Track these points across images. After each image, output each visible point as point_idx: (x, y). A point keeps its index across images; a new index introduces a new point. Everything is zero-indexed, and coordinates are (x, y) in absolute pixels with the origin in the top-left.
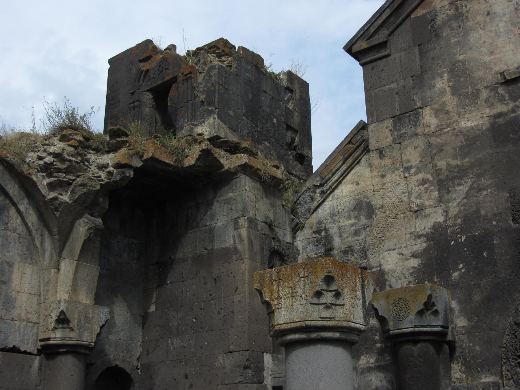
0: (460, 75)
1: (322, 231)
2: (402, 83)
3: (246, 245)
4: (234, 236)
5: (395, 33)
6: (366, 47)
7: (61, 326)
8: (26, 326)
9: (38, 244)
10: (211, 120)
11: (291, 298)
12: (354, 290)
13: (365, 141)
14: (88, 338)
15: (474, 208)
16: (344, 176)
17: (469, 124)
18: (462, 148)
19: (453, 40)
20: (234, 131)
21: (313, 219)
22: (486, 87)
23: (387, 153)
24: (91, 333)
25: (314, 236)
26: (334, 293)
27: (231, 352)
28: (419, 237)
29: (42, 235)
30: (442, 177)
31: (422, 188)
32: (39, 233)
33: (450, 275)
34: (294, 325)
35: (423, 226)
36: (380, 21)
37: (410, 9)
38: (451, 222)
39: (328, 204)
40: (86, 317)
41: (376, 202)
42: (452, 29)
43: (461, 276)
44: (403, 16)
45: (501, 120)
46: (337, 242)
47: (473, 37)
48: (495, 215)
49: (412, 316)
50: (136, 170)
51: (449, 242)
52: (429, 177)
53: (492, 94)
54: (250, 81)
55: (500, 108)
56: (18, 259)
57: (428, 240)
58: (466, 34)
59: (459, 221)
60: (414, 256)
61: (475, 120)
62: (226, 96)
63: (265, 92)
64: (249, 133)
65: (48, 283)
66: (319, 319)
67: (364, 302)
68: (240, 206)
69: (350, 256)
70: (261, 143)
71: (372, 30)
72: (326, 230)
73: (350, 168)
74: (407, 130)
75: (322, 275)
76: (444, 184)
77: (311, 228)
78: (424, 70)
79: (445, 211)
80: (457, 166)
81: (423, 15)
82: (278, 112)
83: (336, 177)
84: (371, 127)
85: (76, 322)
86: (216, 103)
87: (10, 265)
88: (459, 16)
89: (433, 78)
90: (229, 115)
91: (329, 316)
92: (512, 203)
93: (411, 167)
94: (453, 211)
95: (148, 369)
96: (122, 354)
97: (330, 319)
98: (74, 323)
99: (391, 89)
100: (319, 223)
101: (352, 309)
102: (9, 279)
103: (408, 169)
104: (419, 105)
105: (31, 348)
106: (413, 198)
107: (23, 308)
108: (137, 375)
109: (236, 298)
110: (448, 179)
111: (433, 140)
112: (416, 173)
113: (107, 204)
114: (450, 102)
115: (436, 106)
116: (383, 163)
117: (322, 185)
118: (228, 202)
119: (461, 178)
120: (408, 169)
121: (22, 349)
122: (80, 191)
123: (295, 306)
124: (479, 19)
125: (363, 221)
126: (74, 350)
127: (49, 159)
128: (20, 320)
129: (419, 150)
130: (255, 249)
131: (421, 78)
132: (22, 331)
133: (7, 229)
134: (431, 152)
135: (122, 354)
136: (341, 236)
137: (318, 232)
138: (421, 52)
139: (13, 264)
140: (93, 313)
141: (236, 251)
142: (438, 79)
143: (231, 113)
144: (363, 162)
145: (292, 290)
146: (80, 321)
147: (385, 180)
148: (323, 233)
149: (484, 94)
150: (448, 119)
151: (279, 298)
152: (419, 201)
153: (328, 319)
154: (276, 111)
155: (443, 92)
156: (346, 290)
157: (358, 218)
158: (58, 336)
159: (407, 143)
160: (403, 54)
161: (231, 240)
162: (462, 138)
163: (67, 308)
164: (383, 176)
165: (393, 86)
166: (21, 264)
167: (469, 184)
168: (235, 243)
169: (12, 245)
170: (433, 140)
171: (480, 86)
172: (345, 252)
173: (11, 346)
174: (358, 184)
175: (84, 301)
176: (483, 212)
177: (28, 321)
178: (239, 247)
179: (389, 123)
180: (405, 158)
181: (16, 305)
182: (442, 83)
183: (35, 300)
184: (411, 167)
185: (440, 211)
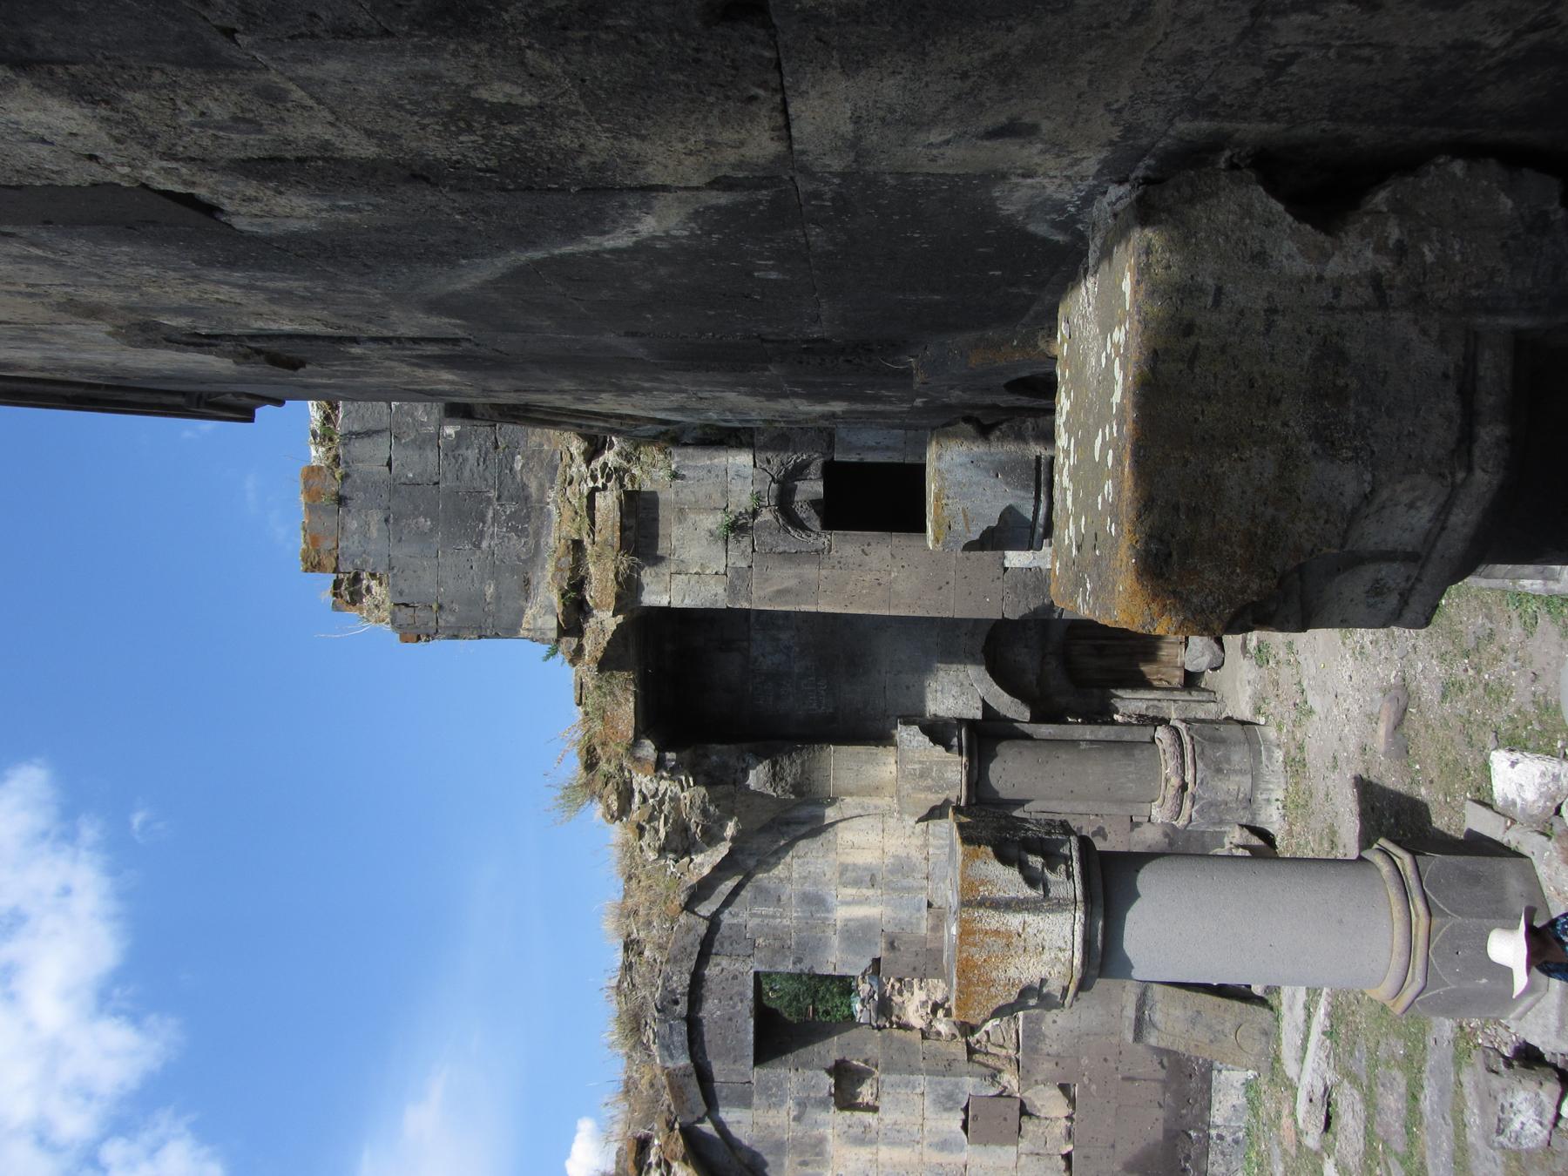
8: (934, 836)
12: (1008, 939)
20: (527, 582)
24: (947, 764)
29: (788, 823)
32: (784, 829)
40: (921, 776)
50: (661, 749)
54: (387, 520)
56: (832, 855)
62: (456, 607)
63: (389, 465)
64: (514, 529)
70: (524, 487)
87: (844, 869)
101: (1046, 957)
102: (866, 869)
107: (906, 842)
113: (719, 747)
128: (926, 845)
130: (792, 583)
133: (789, 879)
140: (912, 762)
143: (490, 590)
146: (929, 789)
154: (422, 424)
156: (1012, 972)
163: (913, 815)
175: (893, 768)
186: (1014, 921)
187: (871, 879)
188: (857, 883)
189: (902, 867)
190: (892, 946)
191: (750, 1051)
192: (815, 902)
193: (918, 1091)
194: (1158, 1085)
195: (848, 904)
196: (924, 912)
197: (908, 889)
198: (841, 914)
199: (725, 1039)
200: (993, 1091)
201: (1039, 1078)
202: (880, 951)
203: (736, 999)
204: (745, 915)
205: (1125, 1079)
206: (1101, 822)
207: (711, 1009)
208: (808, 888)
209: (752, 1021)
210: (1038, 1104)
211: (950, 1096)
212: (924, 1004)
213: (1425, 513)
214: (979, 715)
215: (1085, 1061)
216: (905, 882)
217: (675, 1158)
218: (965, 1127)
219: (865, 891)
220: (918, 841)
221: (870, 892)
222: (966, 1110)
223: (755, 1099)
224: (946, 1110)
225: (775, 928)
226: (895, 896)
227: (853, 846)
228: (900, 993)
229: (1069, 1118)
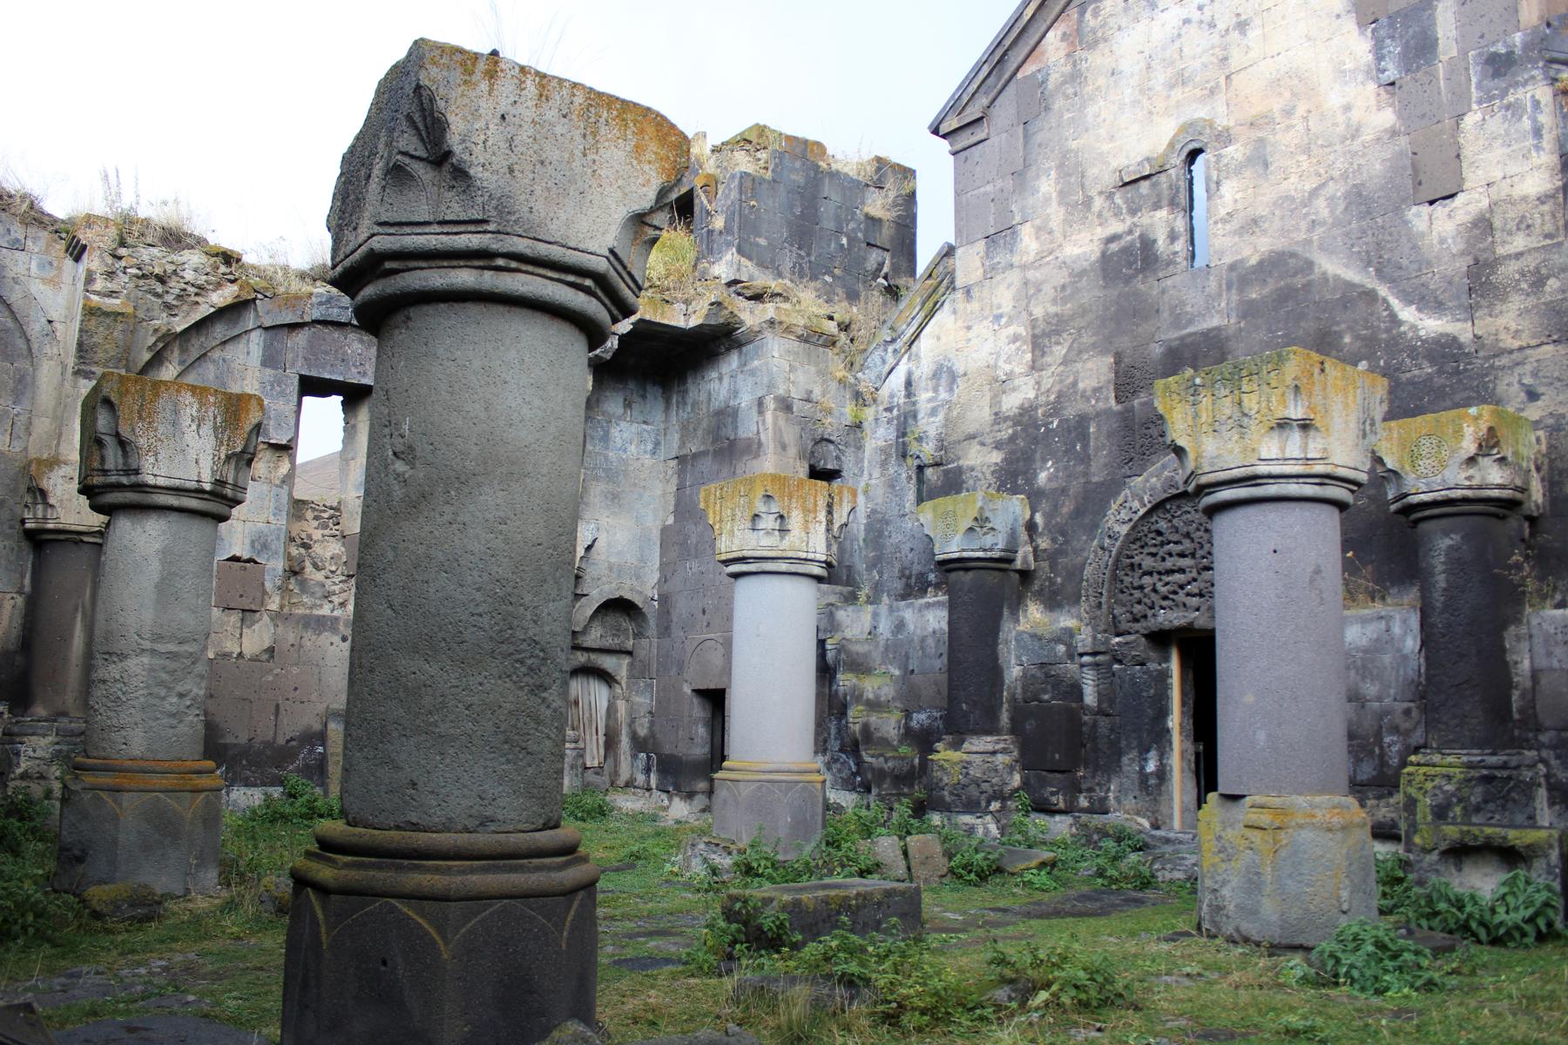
0: (1072, 171)
2: (999, 184)
5: (997, 103)
6: (959, 125)
10: (728, 257)
13: (951, 274)
15: (1071, 379)
16: (921, 328)
17: (1076, 251)
18: (1064, 287)
19: (1067, 116)
22: (1101, 193)
23: (975, 293)
28: (1006, 419)
30: (1037, 331)
31: (1013, 347)
33: (1035, 475)
35: (1011, 403)
36: (974, 86)
37: (1015, 65)
38: (1043, 399)
41: (959, 368)
42: (1067, 97)
43: (1050, 479)
44: (1006, 76)
45: (1114, 247)
47: (1091, 110)
48: (1096, 390)
49: (958, 538)
51: (1038, 428)
52: (1022, 331)
53: (1106, 205)
55: (1116, 227)
57: (1015, 425)
58: (1083, 106)
59: (1052, 398)
60: (998, 446)
61: (1083, 245)
67: (830, 522)
68: (765, 380)
71: (965, 98)
73: (930, 315)
74: (1001, 258)
75: (760, 493)
76: (1039, 343)
78: (1026, 166)
79: (1038, 383)
80: (1057, 315)
81: (1034, 74)
82: (852, 225)
83: (912, 330)
84: (959, 252)
86: (736, 230)
88: (1076, 77)
89: (1038, 177)
90: (758, 245)
92: (1116, 373)
93: (1001, 316)
94: (1047, 383)
97: (771, 548)
99: (986, 194)
100: (892, 396)
103: (998, 317)
104: (1018, 219)
106: (1001, 363)
108: (651, 610)
110: (1044, 334)
111: (1031, 274)
112: (1007, 325)
114: (1056, 214)
115: (1038, 222)
116: (969, 307)
117: (893, 341)
118: (753, 373)
119: (1058, 333)
120: (998, 317)
124: (1101, 81)
125: (943, 395)
129: (1013, 289)
131: (1021, 175)
134: (1029, 291)
137: (889, 410)
138: (1026, 136)
141: (760, 444)
142: (1044, 179)
143: (762, 242)
144: (946, 306)
147: (971, 334)
148: (895, 412)
149: (1098, 203)
150: (1052, 242)
151: (721, 521)
152: (1007, 368)
155: (1047, 200)
157: (936, 390)
159: (999, 278)
160: (1004, 136)
162: (1065, 272)
164: (969, 328)
165: (989, 188)
167: (1067, 345)
170: (1031, 274)
171: (1093, 193)
174: (939, 338)
176: (1081, 386)
179: (981, 246)
180: (995, 302)
182: (1047, 185)
184: (1001, 316)
185: (1031, 381)
186: (822, 516)
191: (314, 373)
193: (271, 518)
194: (270, 736)
199: (326, 353)
200: (268, 585)
201: (280, 630)
205: (277, 706)
209: (341, 378)
210: (256, 627)
211: (265, 546)
212: (310, 537)
213: (1499, 481)
215: (295, 670)
217: (241, 288)
218: (235, 559)
222: (250, 561)
223: (269, 371)
224: (253, 542)
228: (316, 518)
229: (240, 654)
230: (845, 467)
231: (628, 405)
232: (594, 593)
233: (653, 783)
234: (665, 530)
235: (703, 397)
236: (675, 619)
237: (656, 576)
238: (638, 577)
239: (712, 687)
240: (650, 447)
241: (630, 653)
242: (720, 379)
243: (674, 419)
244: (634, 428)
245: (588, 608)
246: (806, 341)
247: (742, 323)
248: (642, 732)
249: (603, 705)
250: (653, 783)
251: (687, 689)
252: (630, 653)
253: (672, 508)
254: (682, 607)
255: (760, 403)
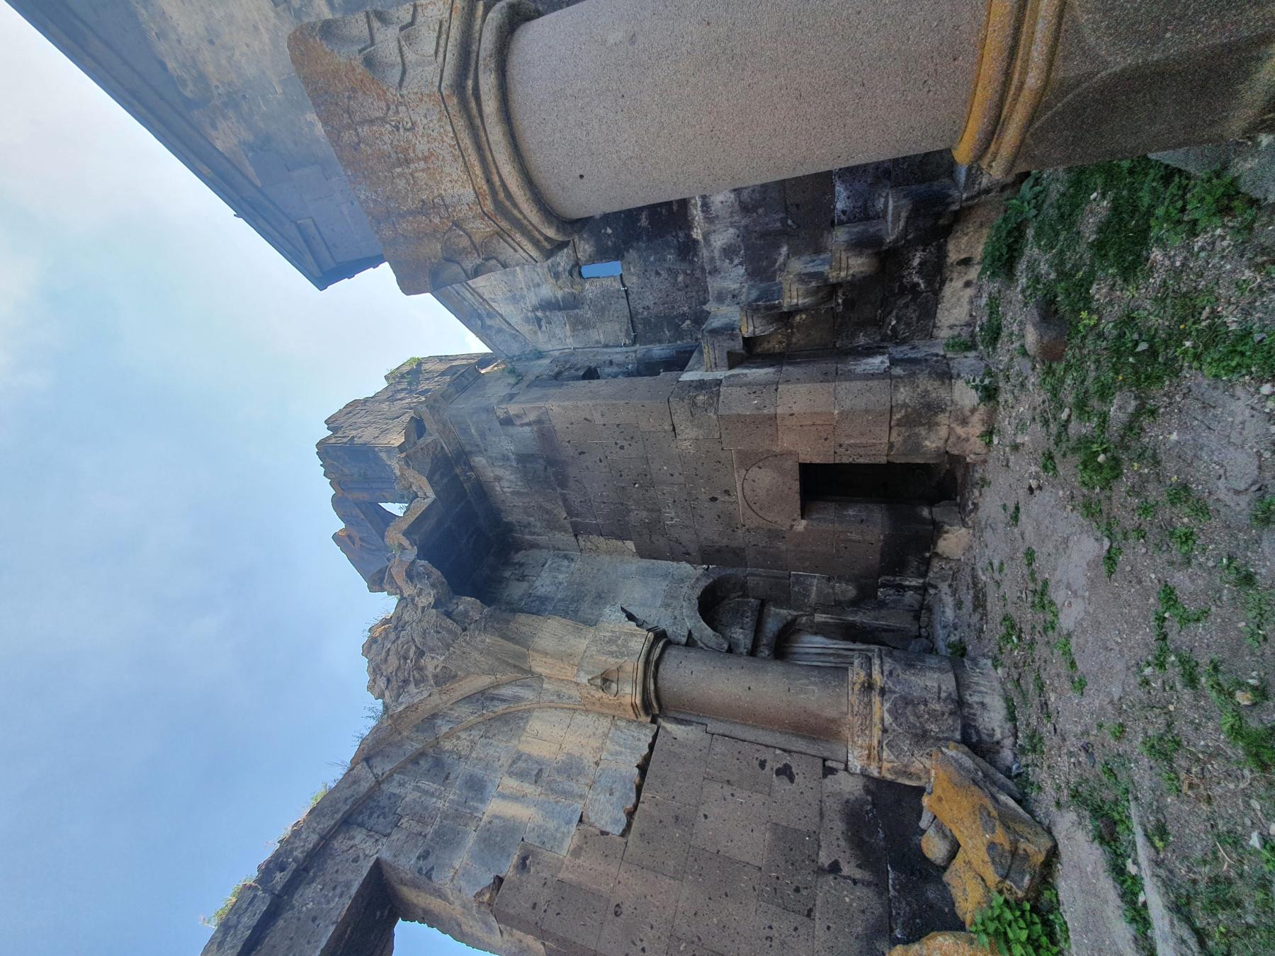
1: (537, 318)
3: (529, 406)
4: (522, 425)
7: (614, 686)
8: (612, 740)
9: (500, 708)
11: (412, 166)
14: (639, 642)
21: (525, 329)
24: (633, 635)
25: (544, 328)
26: (376, 24)
27: (674, 429)
29: (492, 699)
34: (467, 142)
39: (504, 308)
46: (548, 291)
50: (418, 557)
56: (515, 742)
65: (558, 696)
66: (440, 59)
68: (484, 416)
69: (560, 269)
72: (535, 309)
77: (535, 333)
85: (612, 660)
87: (519, 757)
91: (436, 35)
95: (707, 555)
96: (685, 590)
98: (612, 662)
100: (527, 320)
105: (646, 737)
109: (598, 419)
117: (480, 317)
121: (646, 751)
122: (433, 641)
123: (422, 147)
126: (652, 666)
127: (382, 683)
128: (601, 749)
132: (618, 748)
135: (685, 590)
136: (538, 285)
137: (539, 320)
139: (518, 752)
141: (539, 422)
145: (394, 166)
146: (611, 653)
148: (539, 314)
153: (444, 36)
158: (630, 693)
161: (527, 429)
163: (587, 673)
166: (523, 739)
168: (529, 424)
169: (491, 752)
172: (557, 276)
173: (636, 771)
177: (606, 735)
178: (532, 417)
181: (577, 755)
183: (579, 718)
187: (535, 772)
188: (522, 775)
189: (571, 768)
190: (523, 865)
192: (476, 787)
195: (503, 797)
196: (573, 828)
197: (566, 794)
198: (494, 807)
202: (508, 869)
203: (338, 891)
204: (409, 787)
206: (787, 759)
207: (308, 898)
208: (479, 772)
214: (684, 640)
216: (567, 785)
219: (526, 785)
220: (595, 743)
221: (529, 788)
225: (426, 809)
226: (552, 798)
227: (536, 736)
230: (587, 364)
231: (523, 578)
232: (689, 624)
233: (915, 582)
234: (643, 553)
235: (518, 502)
236: (725, 542)
237: (684, 564)
238: (682, 581)
239: (796, 486)
240: (566, 563)
241: (763, 604)
242: (498, 479)
243: (542, 539)
244: (544, 574)
245: (705, 632)
246: (465, 389)
247: (434, 441)
248: (851, 591)
249: (819, 641)
250: (915, 582)
251: (801, 525)
252: (763, 604)
253: (620, 543)
254: (712, 532)
255: (507, 422)
